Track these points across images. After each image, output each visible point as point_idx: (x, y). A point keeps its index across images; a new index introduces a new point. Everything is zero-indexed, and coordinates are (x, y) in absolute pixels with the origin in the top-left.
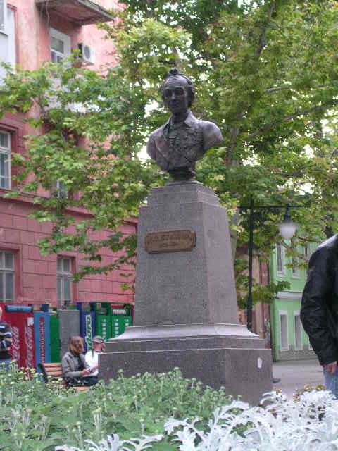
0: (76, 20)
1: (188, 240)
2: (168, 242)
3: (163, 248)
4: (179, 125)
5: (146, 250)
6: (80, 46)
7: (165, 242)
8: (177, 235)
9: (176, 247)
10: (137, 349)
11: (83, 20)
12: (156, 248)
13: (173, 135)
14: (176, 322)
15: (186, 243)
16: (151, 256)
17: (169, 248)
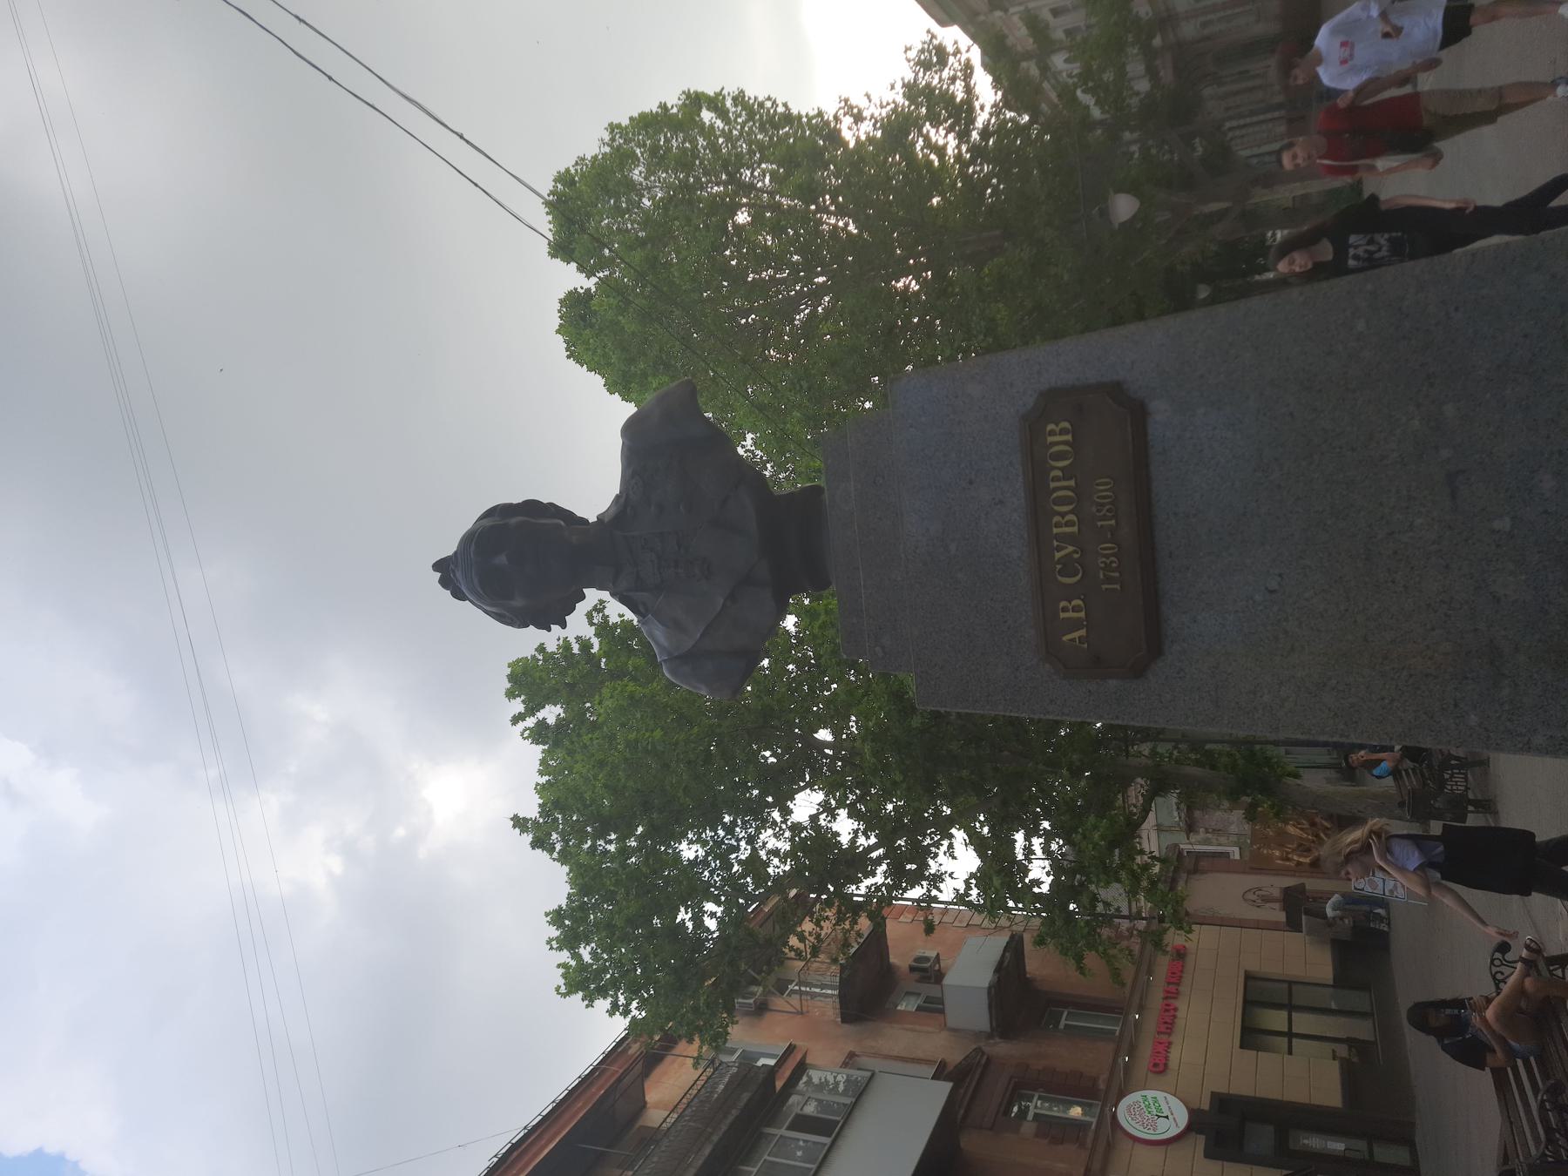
5: (1138, 671)
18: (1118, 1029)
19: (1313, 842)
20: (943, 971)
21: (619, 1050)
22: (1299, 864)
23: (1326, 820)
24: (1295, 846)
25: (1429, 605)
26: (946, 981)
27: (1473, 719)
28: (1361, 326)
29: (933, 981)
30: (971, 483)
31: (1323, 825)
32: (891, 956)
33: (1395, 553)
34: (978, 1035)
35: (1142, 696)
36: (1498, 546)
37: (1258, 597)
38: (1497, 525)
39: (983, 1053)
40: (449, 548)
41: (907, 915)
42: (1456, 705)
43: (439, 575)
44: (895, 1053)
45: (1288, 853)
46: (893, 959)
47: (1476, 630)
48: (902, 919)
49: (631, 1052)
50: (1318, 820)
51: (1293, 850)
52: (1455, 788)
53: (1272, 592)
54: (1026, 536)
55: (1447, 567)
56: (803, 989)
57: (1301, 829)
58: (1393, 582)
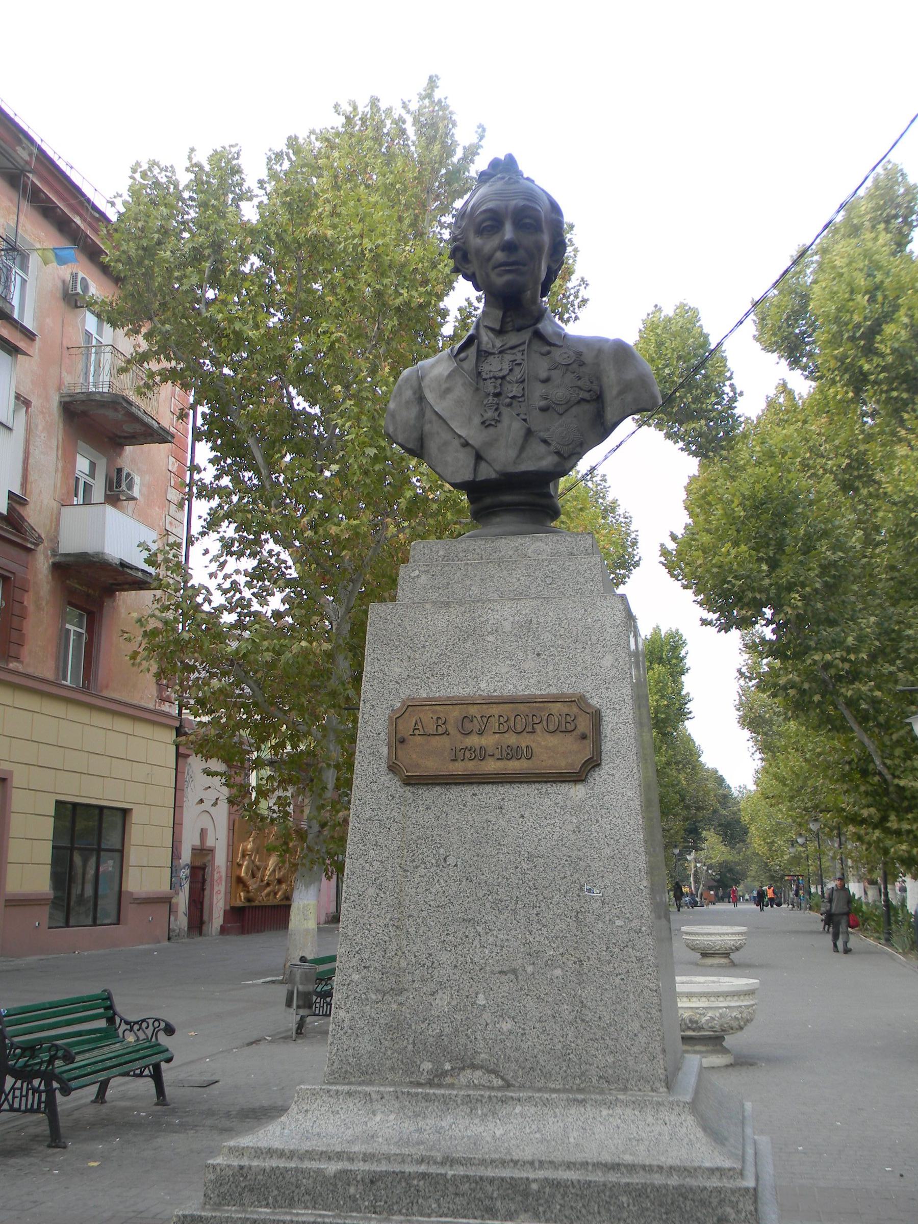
0: (120, 437)
2: (488, 741)
4: (513, 339)
5: (393, 768)
6: (119, 471)
7: (474, 741)
9: (514, 766)
11: (125, 438)
12: (431, 765)
13: (494, 366)
16: (408, 792)
17: (492, 766)
18: (68, 683)
19: (262, 881)
20: (120, 503)
21: (21, 136)
22: (240, 866)
23: (284, 894)
24: (258, 863)
25: (431, 955)
26: (109, 509)
27: (356, 977)
28: (619, 923)
29: (109, 493)
30: (538, 655)
32: (132, 447)
33: (467, 937)
34: (55, 540)
35: (376, 770)
36: (467, 997)
37: (442, 851)
38: (481, 996)
39: (37, 545)
40: (527, 168)
41: (176, 465)
42: (365, 967)
43: (503, 158)
44: (32, 448)
45: (250, 856)
46: (129, 449)
47: (414, 981)
48: (172, 459)
49: (19, 149)
50: (284, 886)
51: (253, 862)
52: (318, 1005)
53: (445, 860)
54: (495, 694)
55: (456, 966)
56: (93, 350)
57: (274, 871)
58: (448, 934)
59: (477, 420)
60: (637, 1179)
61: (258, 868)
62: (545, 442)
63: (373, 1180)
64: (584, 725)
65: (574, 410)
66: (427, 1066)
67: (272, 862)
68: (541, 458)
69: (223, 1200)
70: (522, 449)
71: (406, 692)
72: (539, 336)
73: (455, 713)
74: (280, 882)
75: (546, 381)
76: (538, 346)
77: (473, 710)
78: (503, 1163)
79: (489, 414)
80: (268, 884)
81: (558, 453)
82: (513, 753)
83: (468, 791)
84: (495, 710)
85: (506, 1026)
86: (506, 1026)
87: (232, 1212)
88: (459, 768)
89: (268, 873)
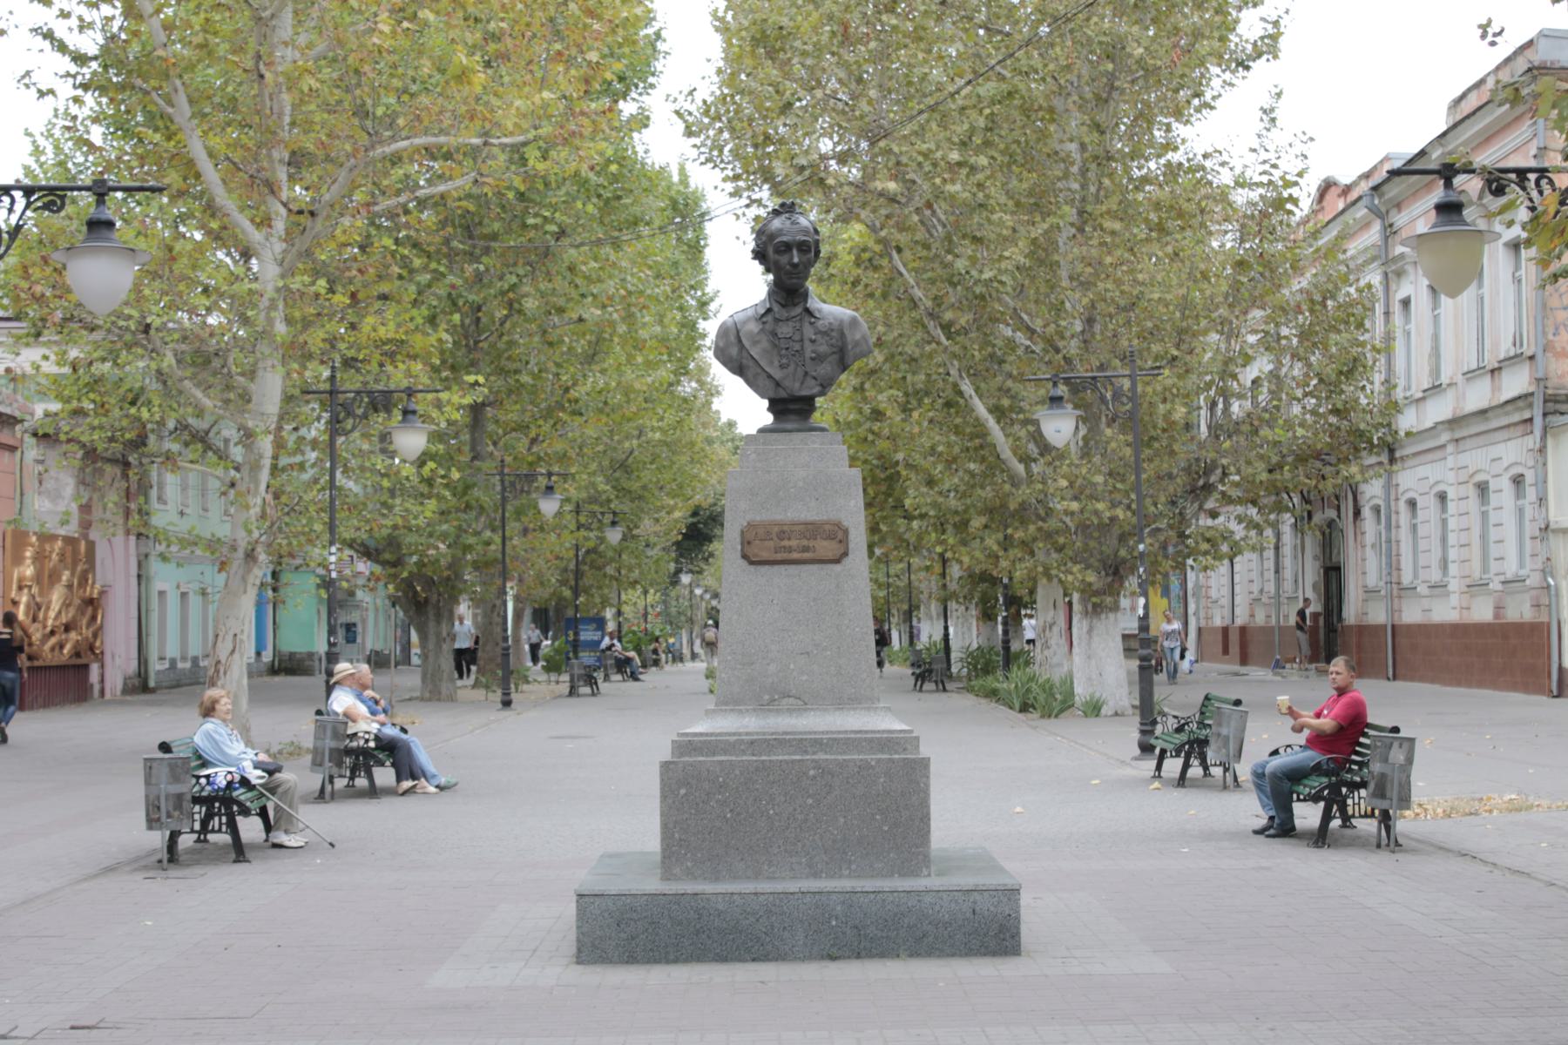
1: (834, 542)
2: (794, 543)
3: (785, 556)
5: (745, 557)
7: (786, 543)
8: (813, 530)
9: (807, 555)
10: (744, 752)
12: (765, 555)
14: (804, 701)
15: (825, 547)
16: (752, 568)
17: (795, 555)
19: (45, 627)
22: (15, 603)
23: (75, 647)
24: (38, 599)
31: (67, 640)
45: (30, 587)
50: (73, 635)
51: (33, 597)
57: (60, 612)
59: (776, 363)
60: (869, 736)
61: (39, 607)
62: (815, 378)
63: (752, 742)
64: (840, 535)
65: (830, 359)
66: (767, 697)
67: (56, 597)
68: (811, 388)
69: (682, 755)
70: (802, 383)
71: (749, 517)
72: (808, 311)
73: (776, 529)
74: (68, 628)
75: (813, 341)
76: (807, 318)
77: (785, 528)
78: (810, 733)
79: (784, 361)
80: (52, 633)
81: (822, 385)
82: (806, 549)
83: (782, 568)
84: (796, 528)
85: (805, 678)
86: (805, 678)
87: (687, 759)
88: (779, 556)
89: (52, 614)
